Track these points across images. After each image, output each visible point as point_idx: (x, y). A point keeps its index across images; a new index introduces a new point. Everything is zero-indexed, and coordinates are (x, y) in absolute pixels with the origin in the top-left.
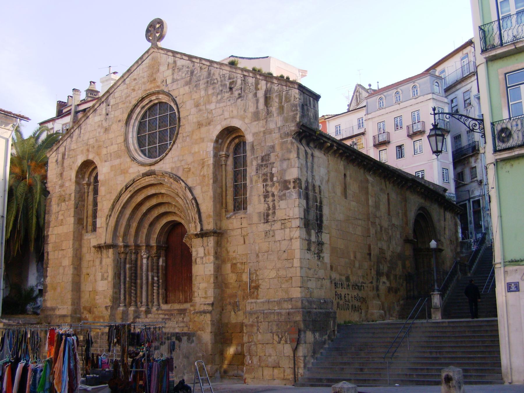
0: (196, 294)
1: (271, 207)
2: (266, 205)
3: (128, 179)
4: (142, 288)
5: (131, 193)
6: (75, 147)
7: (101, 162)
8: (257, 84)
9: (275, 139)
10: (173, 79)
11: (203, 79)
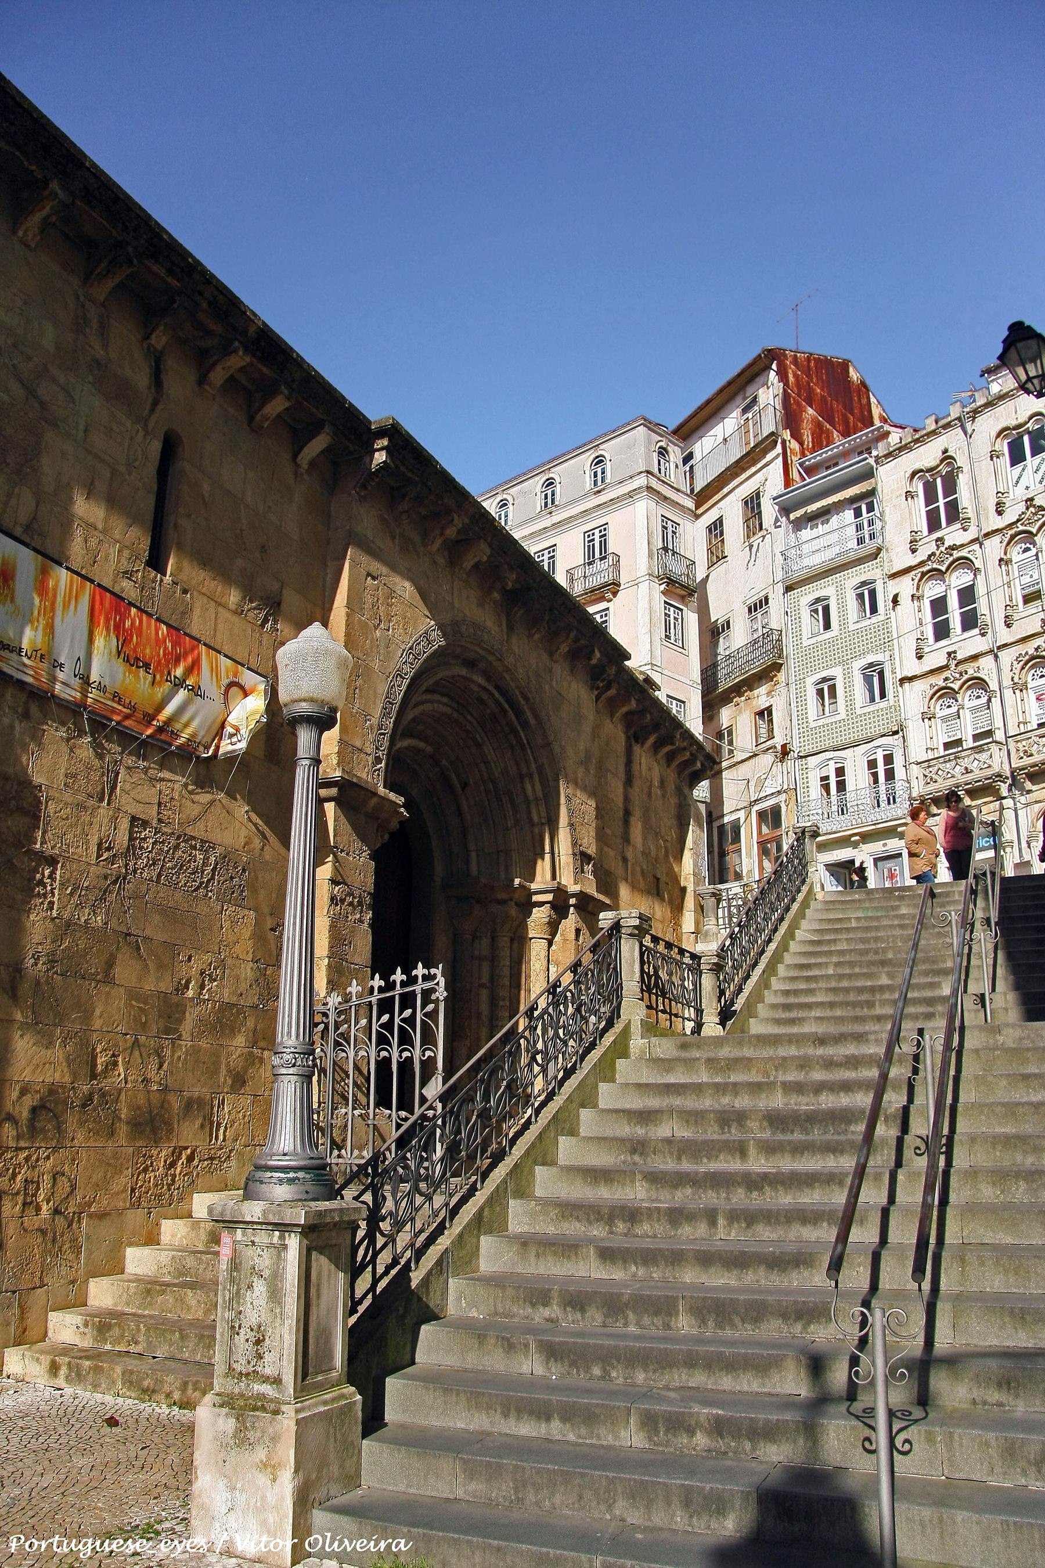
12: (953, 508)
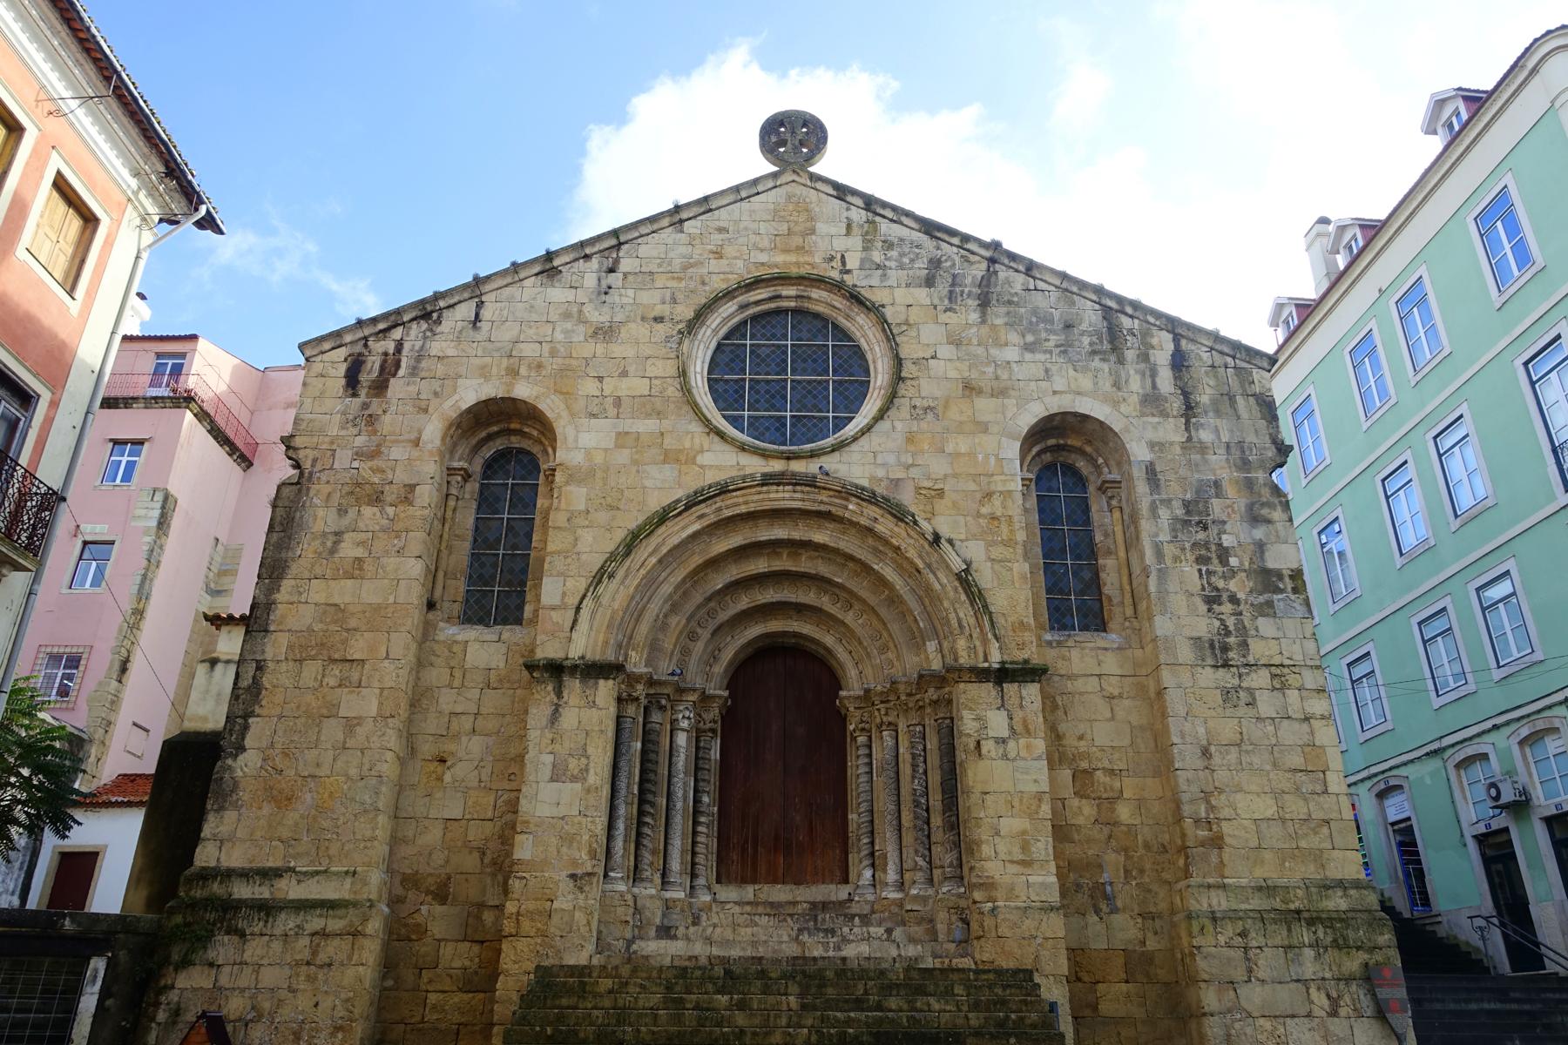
0: (986, 850)
1: (1231, 628)
2: (1217, 623)
3: (693, 481)
5: (706, 522)
6: (450, 352)
7: (572, 415)
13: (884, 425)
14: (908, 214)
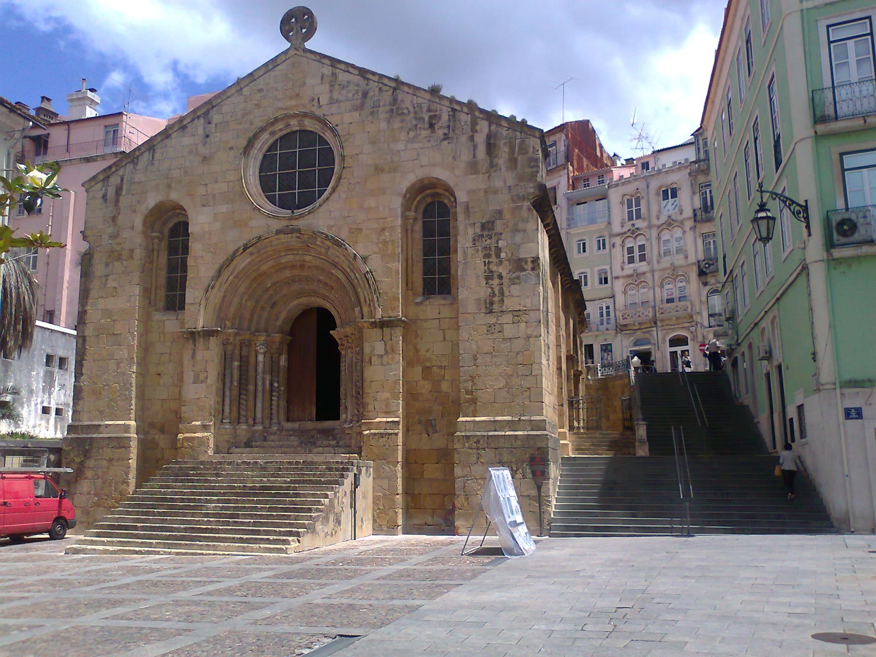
1: (497, 292)
2: (490, 290)
4: (255, 398)
6: (143, 179)
8: (474, 124)
9: (503, 201)
10: (331, 98)
11: (384, 105)
12: (638, 211)
13: (336, 195)
14: (353, 66)
